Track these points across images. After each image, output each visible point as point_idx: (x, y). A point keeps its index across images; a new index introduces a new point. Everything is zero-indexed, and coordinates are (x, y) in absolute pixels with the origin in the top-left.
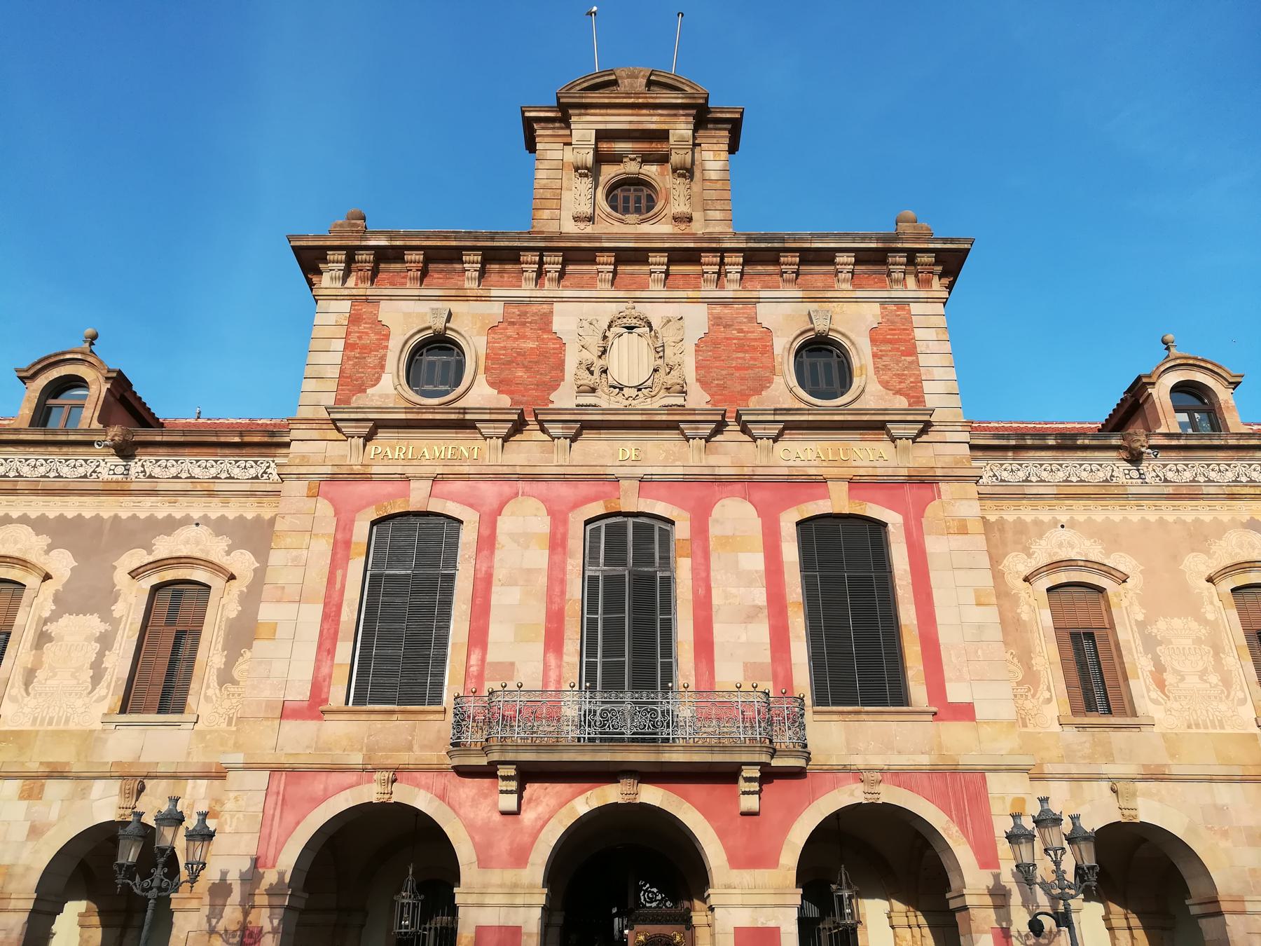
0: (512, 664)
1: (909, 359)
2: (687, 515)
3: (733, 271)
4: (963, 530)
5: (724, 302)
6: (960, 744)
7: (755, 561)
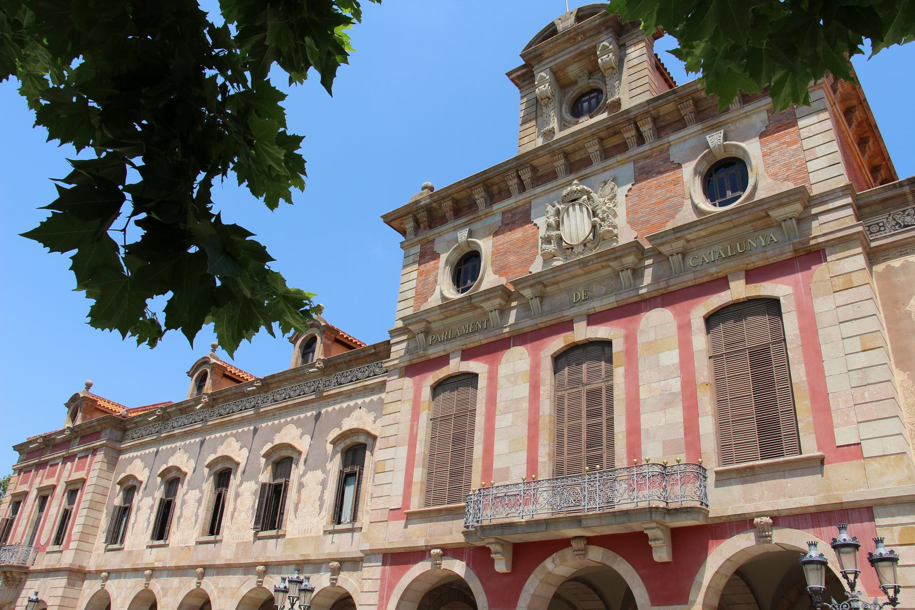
0: (508, 468)
1: (794, 147)
3: (647, 129)
6: (843, 484)
7: (671, 357)
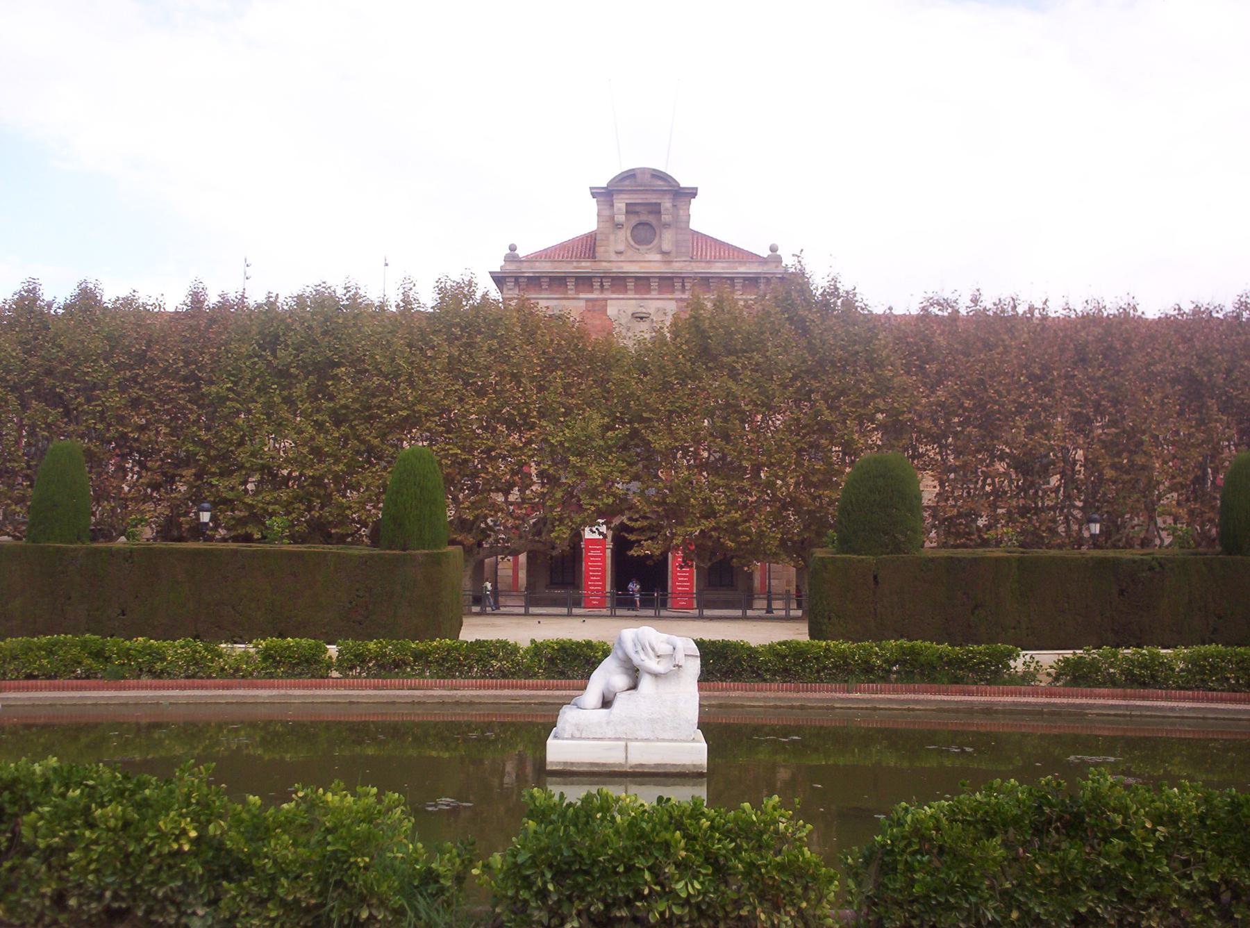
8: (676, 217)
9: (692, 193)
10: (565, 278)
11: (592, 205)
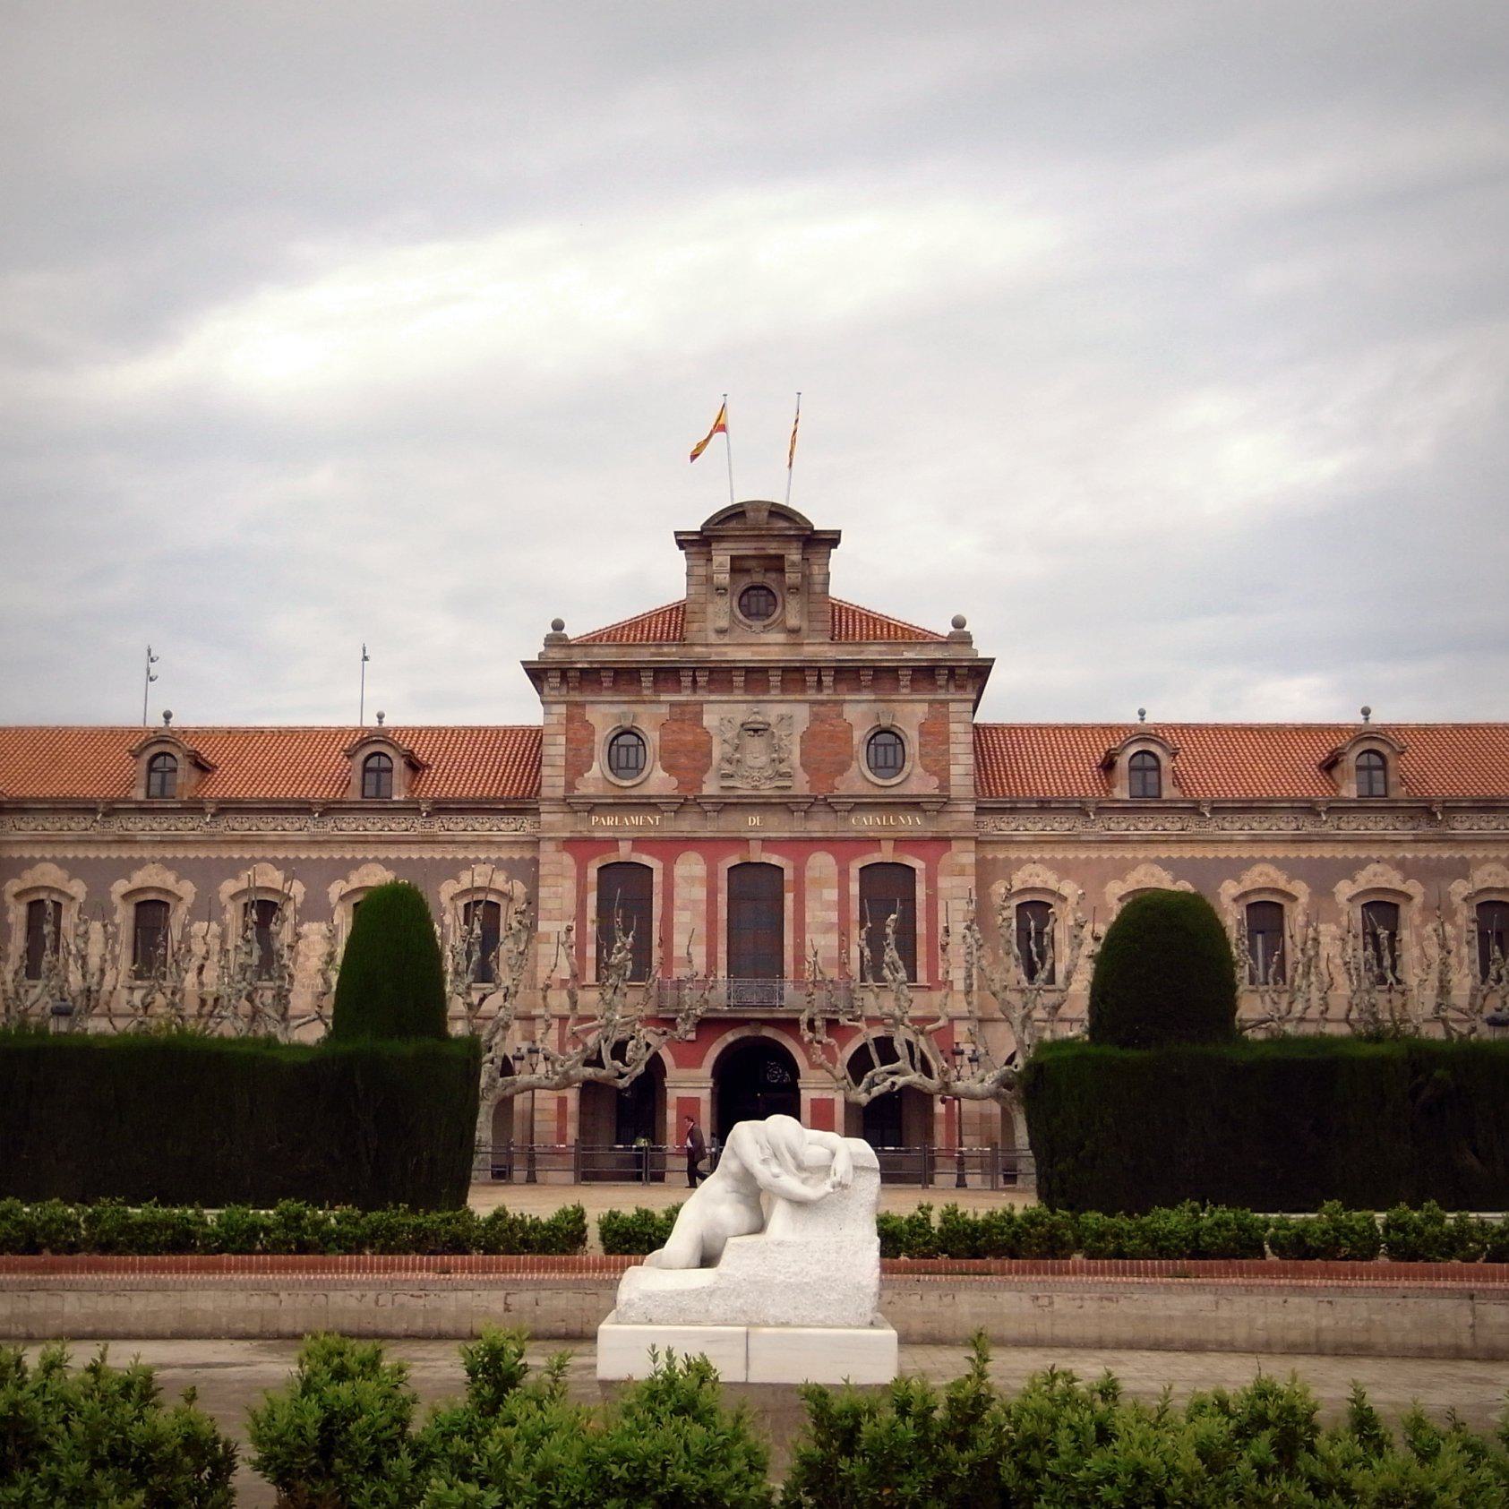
2: (791, 864)
3: (827, 680)
4: (962, 873)
5: (822, 703)
7: (832, 894)
8: (807, 577)
9: (833, 539)
10: (638, 670)
11: (678, 560)
